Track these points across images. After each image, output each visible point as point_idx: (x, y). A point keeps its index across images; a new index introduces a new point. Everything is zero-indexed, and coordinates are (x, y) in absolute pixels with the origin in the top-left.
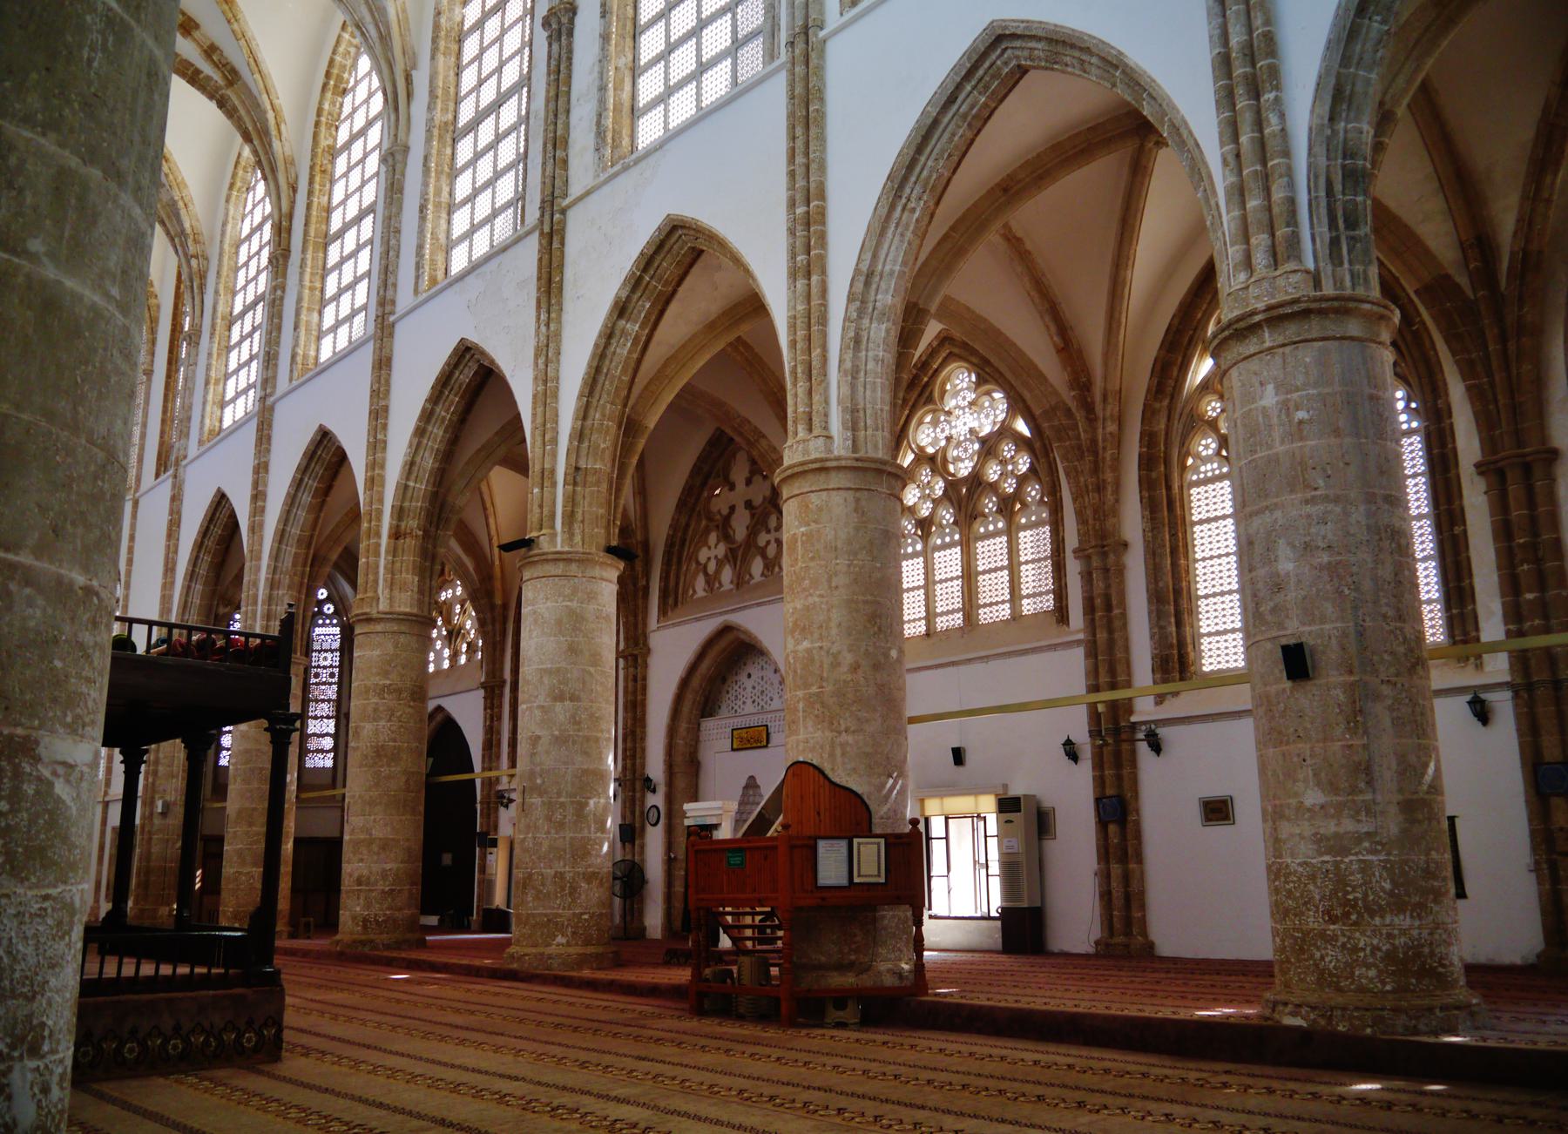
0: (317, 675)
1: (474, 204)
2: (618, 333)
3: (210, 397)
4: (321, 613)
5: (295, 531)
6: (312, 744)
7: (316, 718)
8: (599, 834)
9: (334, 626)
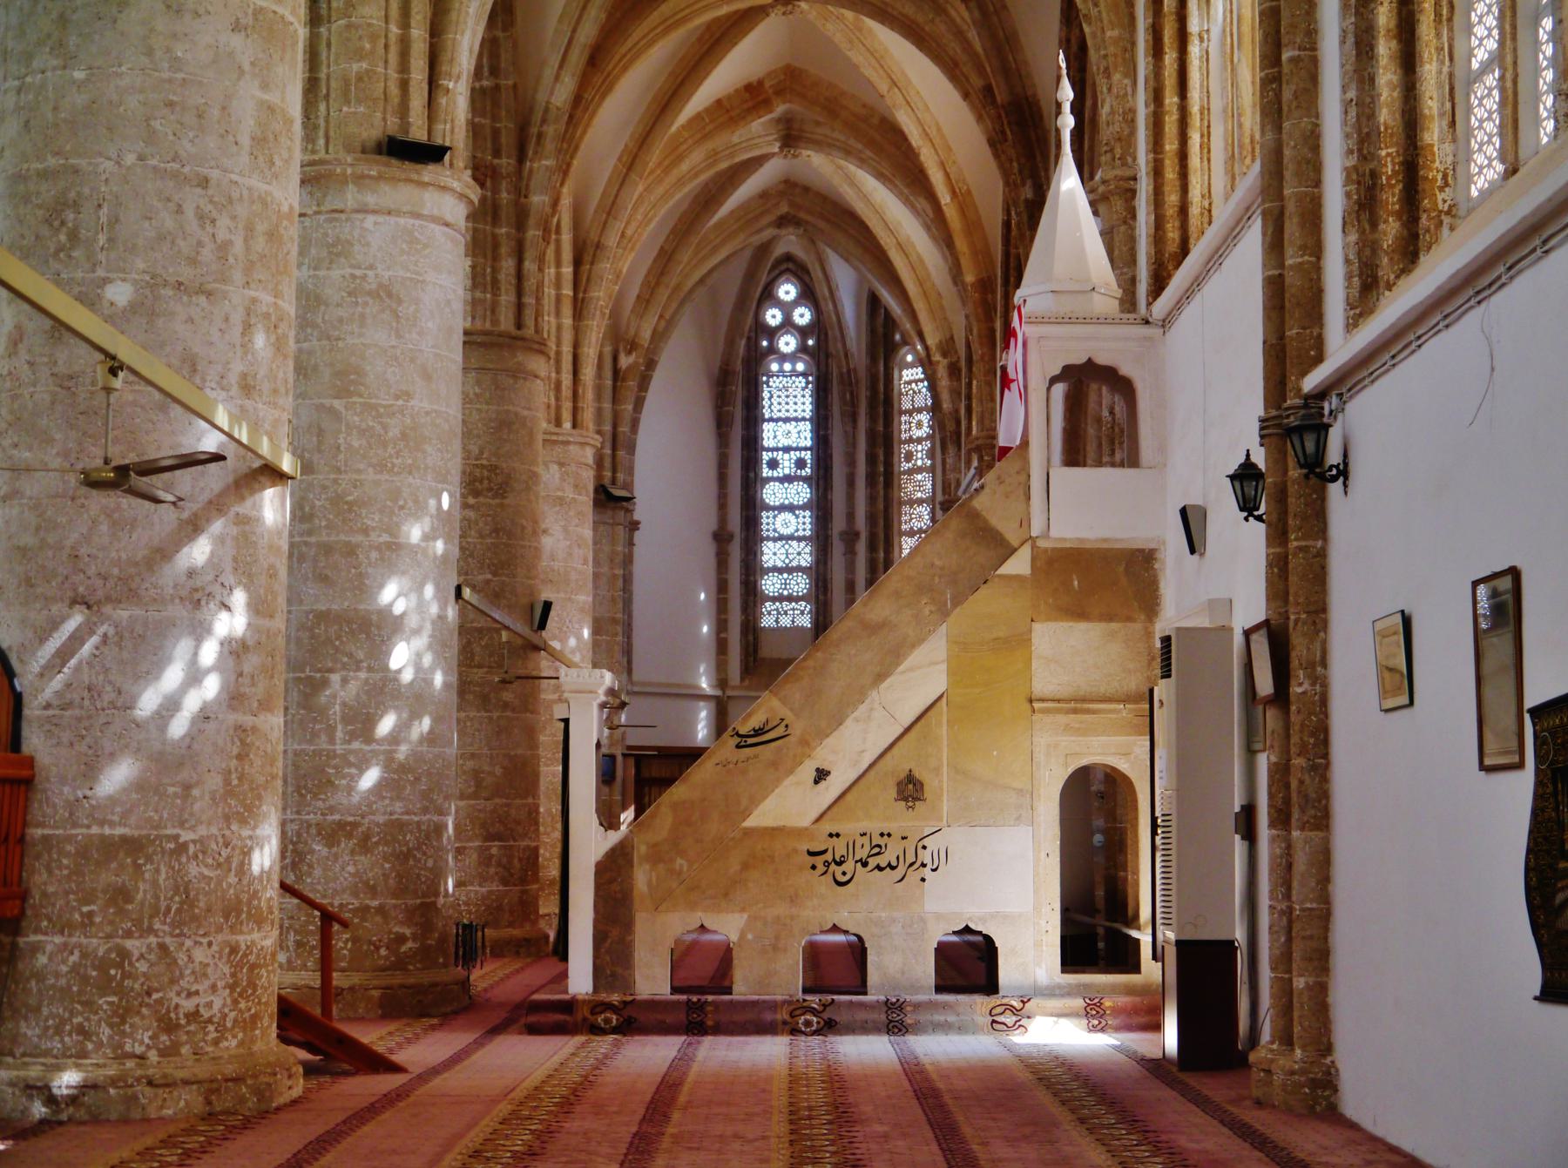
8: (356, 745)
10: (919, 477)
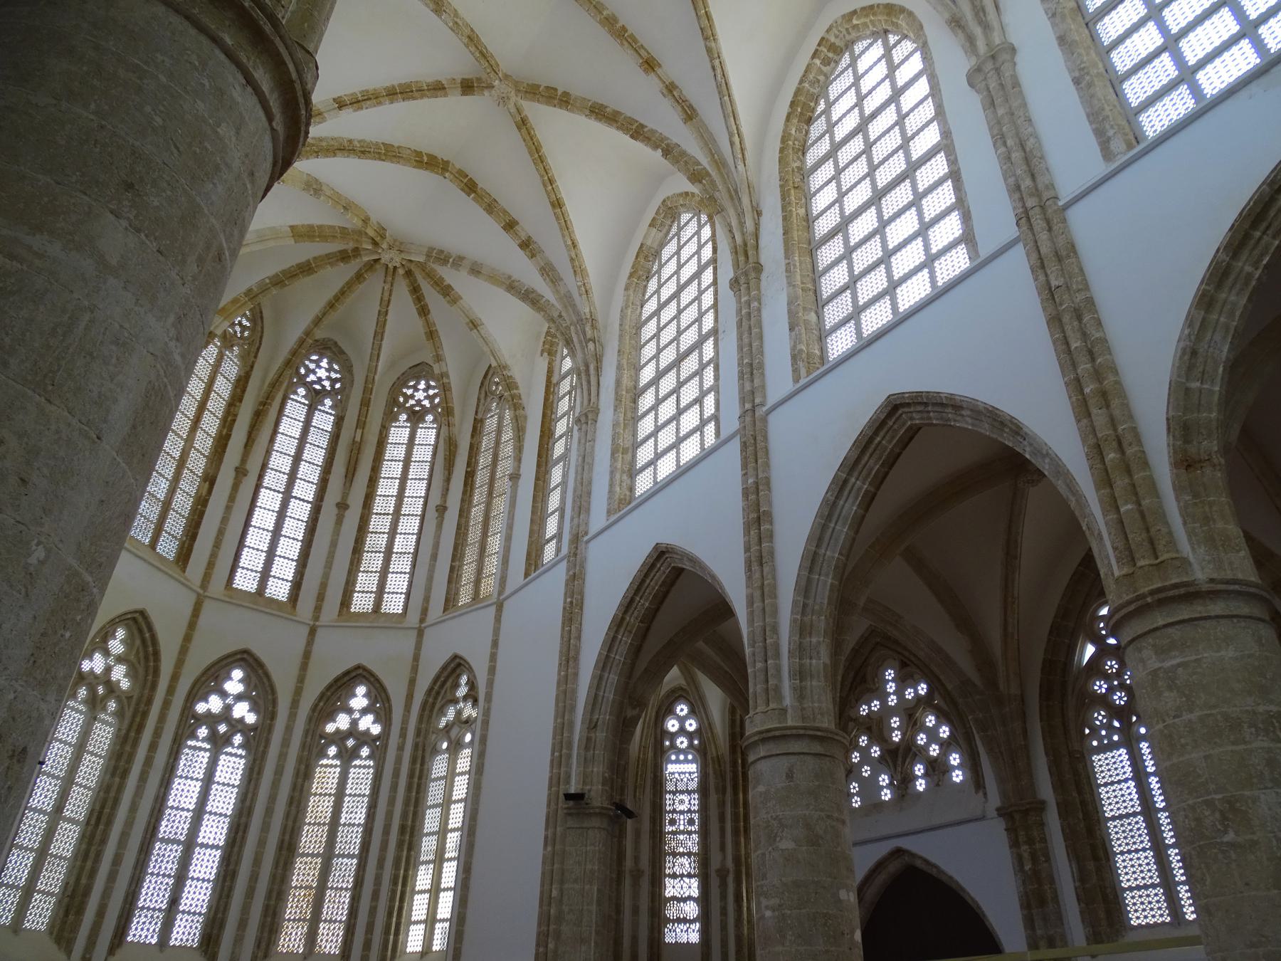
0: (673, 822)
1: (656, 466)
3: (619, 465)
4: (673, 746)
5: (832, 554)
6: (671, 911)
7: (674, 876)
9: (686, 761)
10: (681, 837)
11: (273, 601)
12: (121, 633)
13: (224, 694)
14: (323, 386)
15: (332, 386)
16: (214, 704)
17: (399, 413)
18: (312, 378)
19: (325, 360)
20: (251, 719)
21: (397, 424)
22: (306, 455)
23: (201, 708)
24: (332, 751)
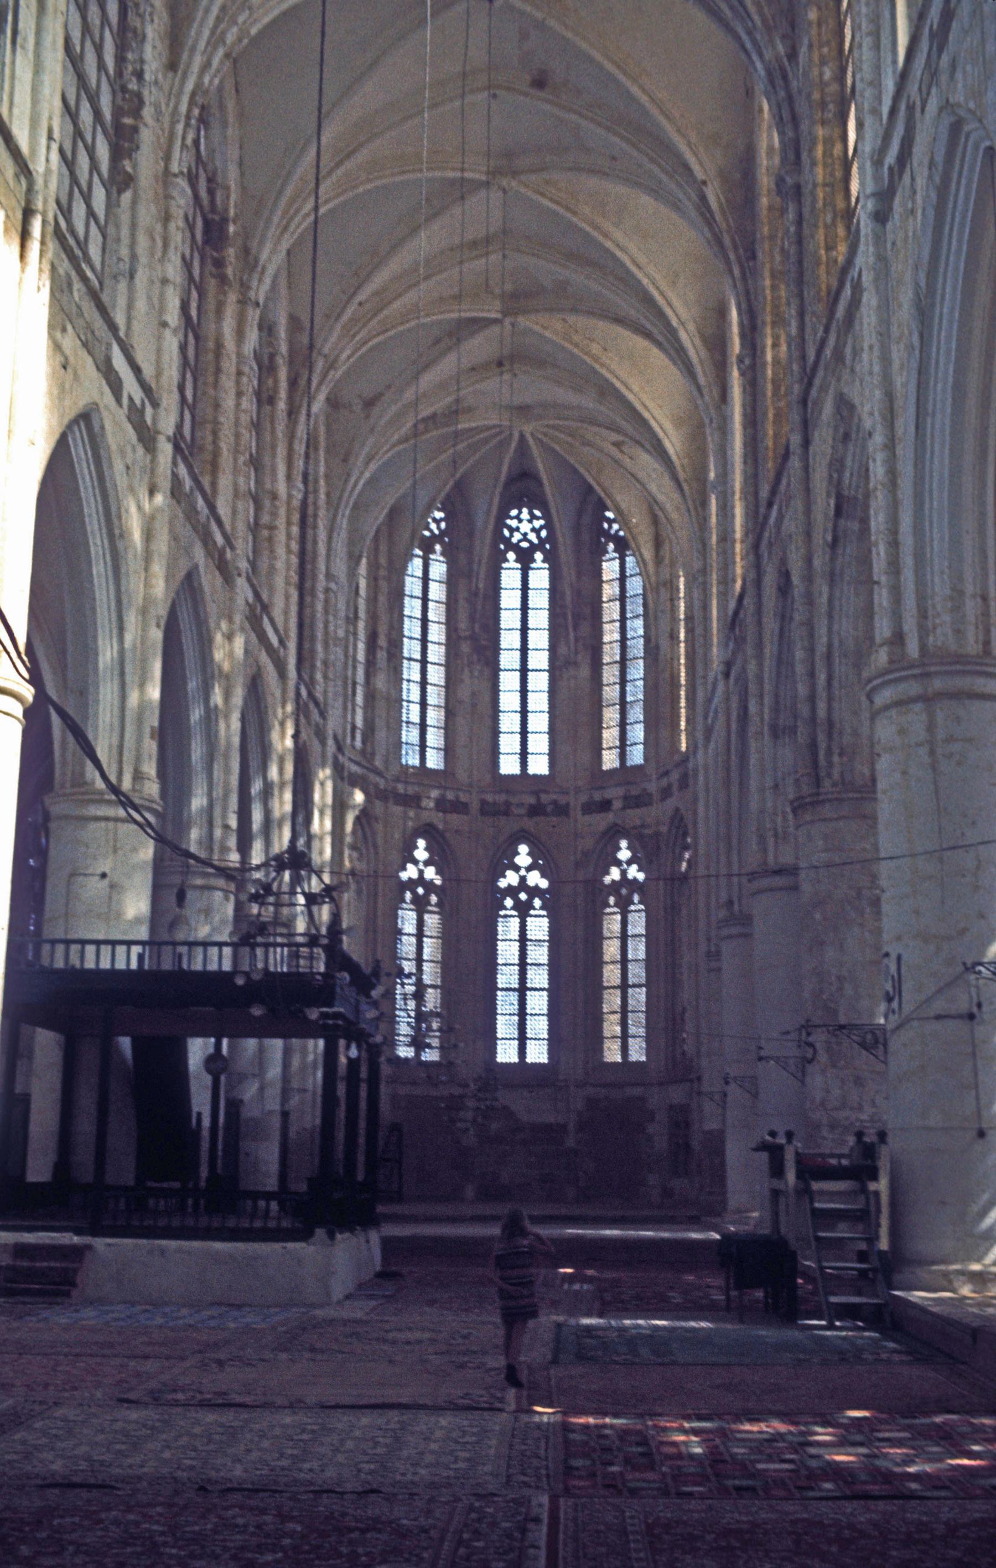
2: (840, 534)
11: (535, 776)
12: (421, 843)
13: (517, 869)
14: (530, 542)
15: (538, 537)
16: (511, 878)
17: (606, 544)
18: (517, 537)
19: (525, 511)
20: (544, 884)
21: (608, 556)
22: (531, 623)
23: (503, 883)
24: (612, 900)
